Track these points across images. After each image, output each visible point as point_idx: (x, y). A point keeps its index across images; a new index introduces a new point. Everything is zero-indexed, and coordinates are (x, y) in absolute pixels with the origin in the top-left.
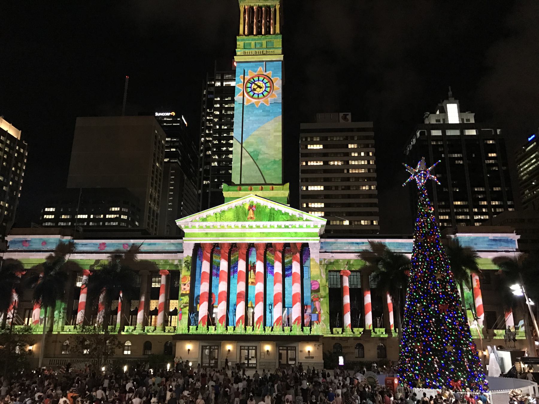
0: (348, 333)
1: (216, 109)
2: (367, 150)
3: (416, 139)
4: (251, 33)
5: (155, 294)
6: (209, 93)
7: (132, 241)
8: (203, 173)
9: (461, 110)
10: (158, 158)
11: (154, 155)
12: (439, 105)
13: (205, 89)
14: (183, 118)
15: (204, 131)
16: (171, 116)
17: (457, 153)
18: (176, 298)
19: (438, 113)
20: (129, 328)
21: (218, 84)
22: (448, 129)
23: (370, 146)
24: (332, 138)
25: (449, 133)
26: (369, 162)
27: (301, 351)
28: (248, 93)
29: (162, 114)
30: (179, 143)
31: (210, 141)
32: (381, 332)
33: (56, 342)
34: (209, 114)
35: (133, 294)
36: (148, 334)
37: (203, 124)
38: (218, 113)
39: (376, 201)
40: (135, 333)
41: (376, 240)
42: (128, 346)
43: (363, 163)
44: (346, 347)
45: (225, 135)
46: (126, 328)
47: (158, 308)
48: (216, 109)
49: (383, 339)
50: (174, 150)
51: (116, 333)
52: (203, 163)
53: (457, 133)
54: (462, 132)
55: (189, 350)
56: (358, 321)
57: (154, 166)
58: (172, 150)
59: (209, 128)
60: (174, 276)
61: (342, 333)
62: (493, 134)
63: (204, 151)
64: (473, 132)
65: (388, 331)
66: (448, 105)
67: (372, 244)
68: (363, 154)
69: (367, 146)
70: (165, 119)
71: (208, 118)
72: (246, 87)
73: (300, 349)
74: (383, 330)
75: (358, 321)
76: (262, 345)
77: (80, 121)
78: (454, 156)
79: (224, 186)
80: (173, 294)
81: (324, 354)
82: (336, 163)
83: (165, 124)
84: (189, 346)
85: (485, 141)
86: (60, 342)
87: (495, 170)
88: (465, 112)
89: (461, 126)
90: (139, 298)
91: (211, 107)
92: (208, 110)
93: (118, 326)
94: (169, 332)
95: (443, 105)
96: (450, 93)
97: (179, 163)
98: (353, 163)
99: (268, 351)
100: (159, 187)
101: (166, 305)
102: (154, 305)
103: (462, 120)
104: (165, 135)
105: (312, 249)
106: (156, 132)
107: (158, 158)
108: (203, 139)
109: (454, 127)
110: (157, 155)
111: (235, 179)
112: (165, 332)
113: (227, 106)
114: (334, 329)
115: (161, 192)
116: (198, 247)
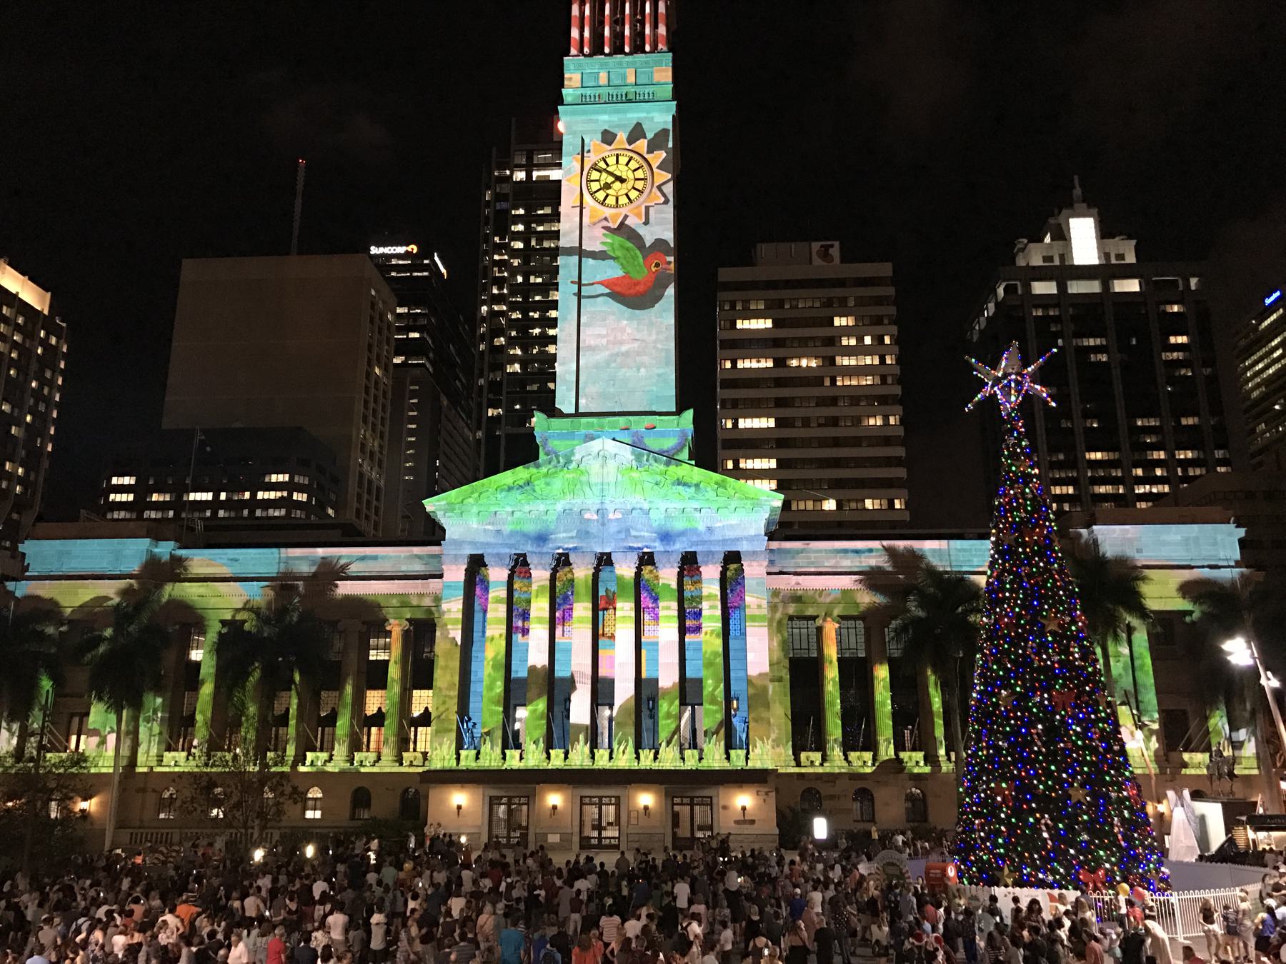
1: (517, 236)
2: (878, 330)
3: (997, 305)
4: (597, 50)
5: (376, 676)
6: (498, 197)
7: (321, 552)
8: (485, 390)
9: (1104, 233)
11: (370, 347)
12: (1052, 221)
14: (436, 258)
15: (486, 288)
16: (407, 255)
17: (1095, 336)
18: (428, 685)
19: (1048, 239)
20: (317, 758)
21: (520, 175)
23: (886, 321)
24: (794, 303)
25: (1075, 287)
27: (725, 808)
28: (592, 194)
30: (429, 321)
31: (502, 313)
32: (914, 760)
33: (143, 790)
34: (498, 248)
35: (325, 676)
36: (363, 770)
37: (486, 272)
38: (519, 245)
39: (900, 452)
40: (330, 768)
41: (901, 544)
42: (316, 799)
43: (868, 360)
44: (832, 797)
45: (538, 298)
46: (310, 756)
48: (517, 236)
49: (918, 778)
50: (417, 335)
51: (287, 769)
52: (486, 366)
53: (1094, 287)
54: (1106, 286)
55: (459, 807)
57: (369, 374)
59: (500, 282)
60: (422, 631)
61: (822, 765)
62: (1181, 288)
63: (487, 337)
64: (1133, 286)
65: (931, 759)
66: (1071, 220)
67: (891, 552)
68: (868, 340)
69: (878, 321)
70: (394, 262)
71: (496, 257)
72: (589, 181)
73: (722, 803)
75: (859, 733)
77: (190, 270)
78: (1086, 344)
79: (538, 420)
80: (421, 675)
81: (780, 814)
82: (804, 363)
83: (393, 274)
84: (460, 798)
85: (1162, 307)
86: (154, 791)
87: (1186, 377)
88: (1114, 237)
90: (338, 686)
91: (503, 230)
92: (497, 239)
93: (291, 751)
94: (411, 765)
95: (1061, 219)
96: (1078, 192)
97: (428, 365)
98: (846, 361)
99: (646, 808)
101: (406, 701)
102: (374, 701)
103: (1107, 256)
104: (394, 300)
109: (1086, 272)
110: (375, 349)
111: (565, 402)
112: (401, 764)
113: (540, 229)
114: (803, 755)
115: (387, 434)
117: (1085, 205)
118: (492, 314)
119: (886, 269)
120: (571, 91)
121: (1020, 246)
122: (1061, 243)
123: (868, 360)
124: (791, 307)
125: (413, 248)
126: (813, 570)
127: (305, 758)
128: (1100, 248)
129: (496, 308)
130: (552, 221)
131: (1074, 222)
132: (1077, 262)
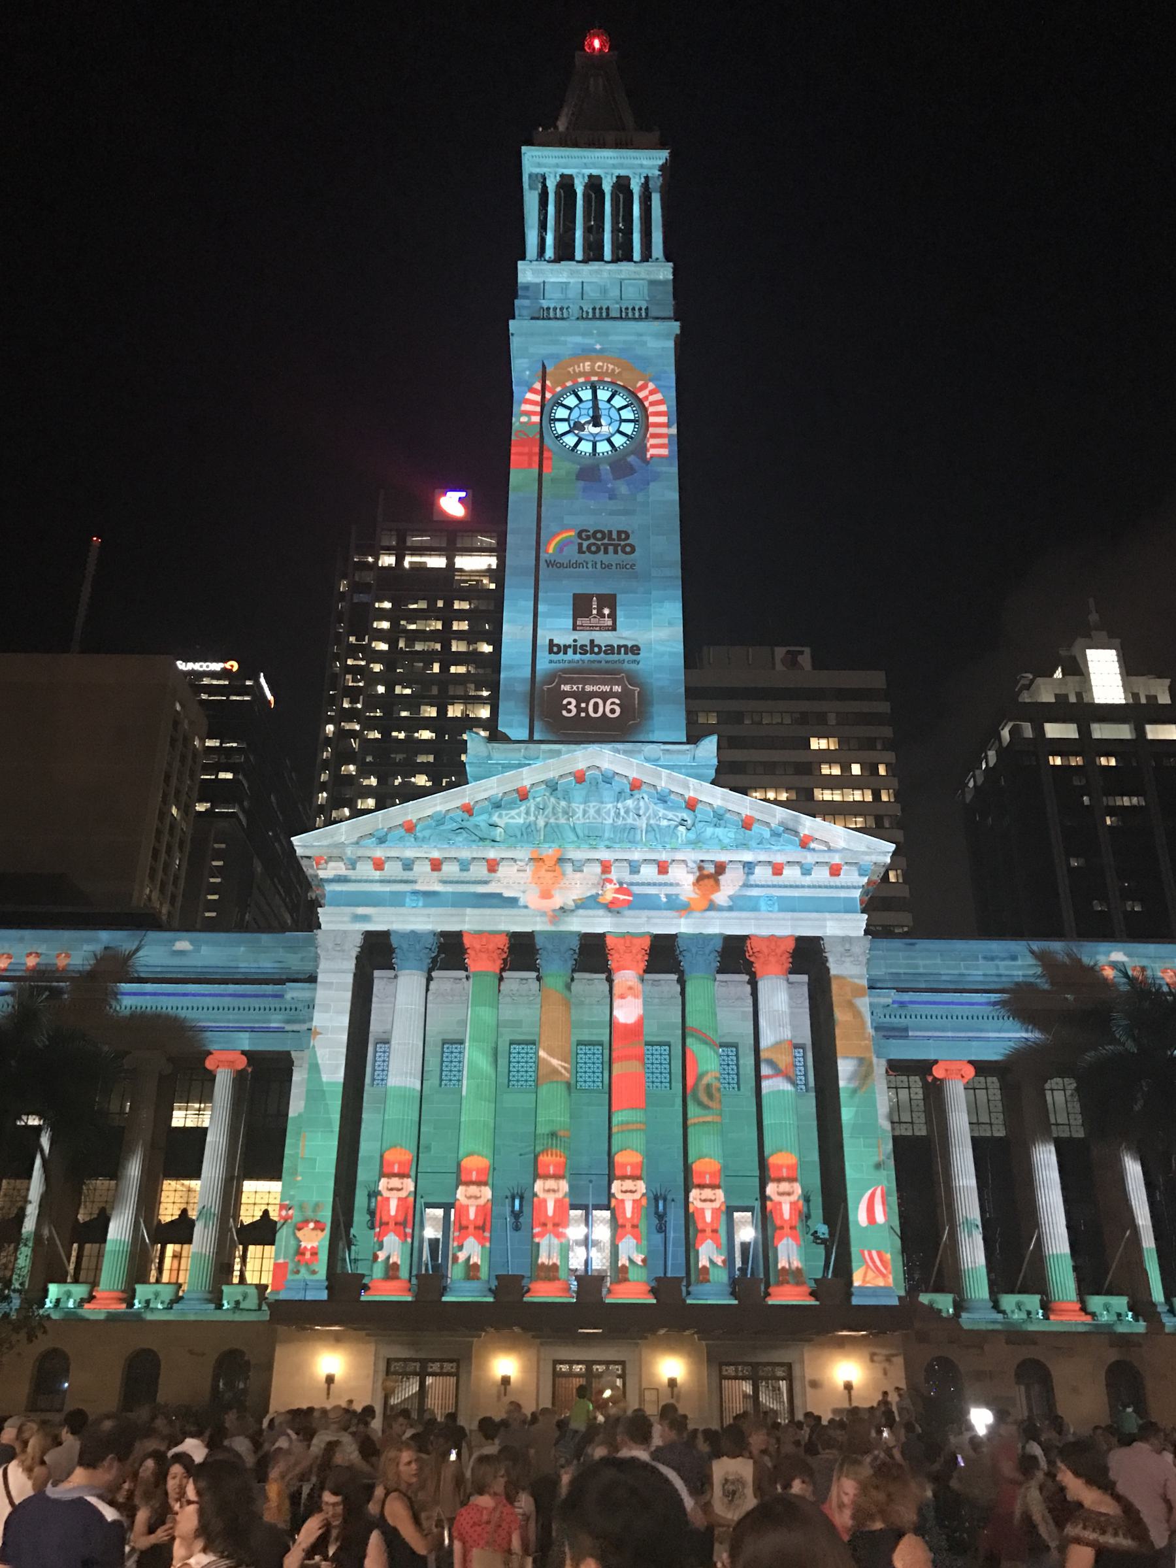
1: (380, 635)
2: (871, 755)
4: (564, 253)
5: (183, 1153)
6: (355, 587)
7: (105, 937)
9: (1129, 669)
10: (178, 792)
11: (167, 778)
13: (345, 578)
14: (262, 680)
15: (334, 701)
16: (225, 673)
17: (1130, 795)
18: (274, 1173)
19: (1058, 674)
21: (388, 560)
25: (1101, 731)
26: (877, 796)
27: (815, 1384)
29: (197, 666)
30: (247, 758)
31: (353, 734)
32: (1111, 1308)
34: (353, 651)
35: (89, 1156)
36: (149, 1317)
37: (335, 680)
38: (383, 646)
41: (1057, 947)
43: (857, 796)
45: (404, 714)
46: (54, 1290)
47: (193, 1214)
48: (380, 635)
49: (1125, 1341)
50: (229, 776)
53: (1123, 732)
54: (1141, 732)
55: (330, 1379)
56: (1015, 1263)
57: (164, 814)
58: (223, 775)
59: (353, 694)
60: (265, 1085)
65: (1141, 1307)
66: (1088, 652)
68: (856, 769)
69: (869, 744)
70: (206, 681)
71: (350, 662)
73: (810, 1374)
74: (1120, 1303)
75: (1015, 1263)
76: (646, 1353)
78: (1119, 803)
80: (260, 1151)
83: (204, 697)
89: (1136, 712)
90: (114, 1172)
91: (362, 626)
92: (352, 639)
95: (1075, 651)
96: (1094, 618)
97: (241, 816)
98: (827, 795)
100: (175, 883)
101: (231, 1197)
102: (174, 1198)
103: (1135, 696)
106: (178, 708)
107: (178, 792)
108: (330, 728)
109: (1109, 713)
110: (174, 781)
112: (219, 1306)
113: (413, 627)
117: (1103, 634)
118: (342, 734)
119: (876, 679)
120: (526, 302)
121: (1023, 682)
122: (1077, 678)
123: (857, 796)
125: (234, 665)
126: (923, 986)
129: (348, 726)
130: (427, 618)
131: (1092, 654)
132: (1097, 701)
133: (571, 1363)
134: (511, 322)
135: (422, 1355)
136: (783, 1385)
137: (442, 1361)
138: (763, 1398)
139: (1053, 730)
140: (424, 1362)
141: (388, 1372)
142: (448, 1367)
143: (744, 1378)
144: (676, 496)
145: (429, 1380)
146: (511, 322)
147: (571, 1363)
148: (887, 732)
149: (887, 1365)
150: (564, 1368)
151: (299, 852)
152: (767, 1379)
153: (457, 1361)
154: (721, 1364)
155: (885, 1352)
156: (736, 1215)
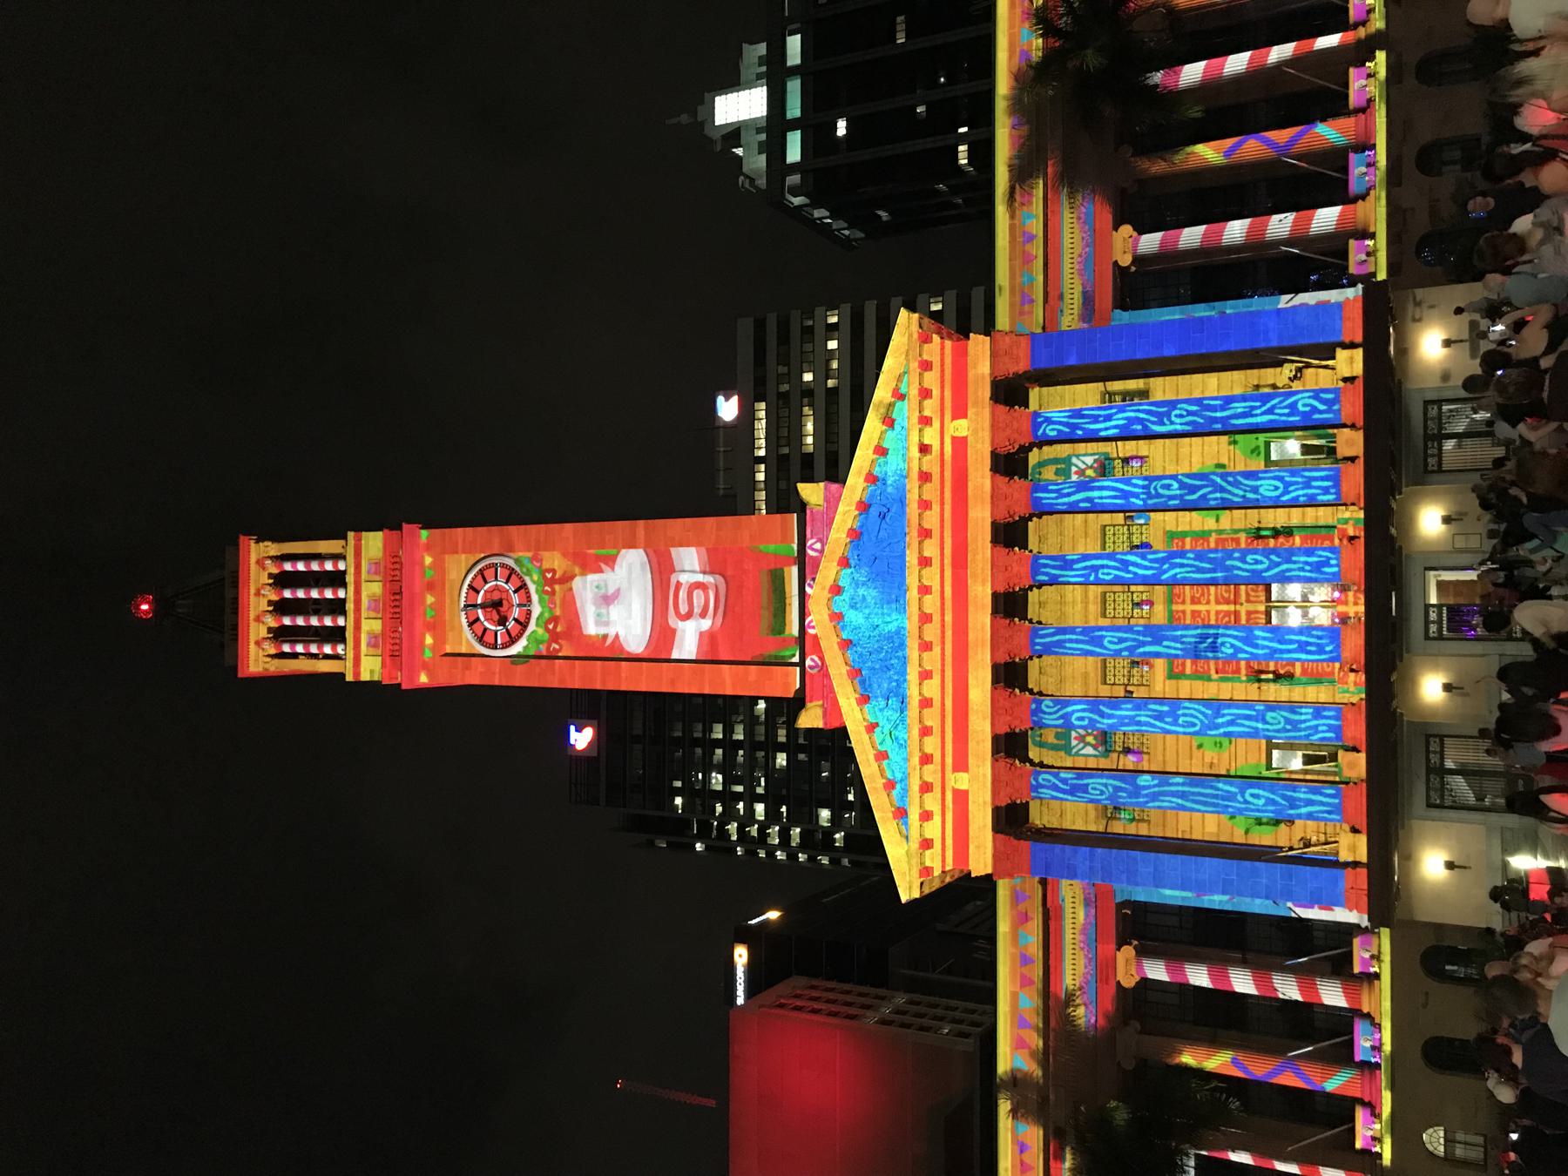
0: (1376, 212)
2: (820, 331)
3: (815, 204)
9: (733, 83)
19: (739, 151)
22: (784, 113)
24: (783, 442)
25: (794, 110)
27: (1446, 377)
36: (1387, 1048)
42: (1449, 1141)
53: (794, 87)
54: (794, 71)
55: (1450, 865)
64: (794, 43)
65: (1360, 53)
67: (1022, 174)
69: (808, 332)
71: (734, 838)
73: (1435, 382)
75: (1323, 180)
84: (1432, 864)
94: (1377, 958)
95: (716, 136)
96: (684, 118)
99: (1447, 520)
103: (759, 77)
105: (1017, 360)
109: (777, 101)
112: (1377, 976)
116: (1011, 819)
118: (803, 846)
124: (788, 445)
127: (1366, 1152)
128: (750, 86)
133: (1427, 622)
134: (404, 687)
135: (1423, 772)
136: (1445, 408)
137: (1428, 751)
138: (1460, 429)
139: (794, 154)
140: (1429, 771)
141: (1441, 807)
142: (1434, 747)
143: (1440, 449)
144: (568, 526)
145: (1449, 764)
146: (404, 687)
147: (1427, 622)
148: (795, 315)
149: (1424, 306)
150: (1433, 628)
151: (916, 895)
152: (1440, 428)
153: (1428, 737)
154: (1426, 471)
155: (1410, 308)
156: (1274, 457)
